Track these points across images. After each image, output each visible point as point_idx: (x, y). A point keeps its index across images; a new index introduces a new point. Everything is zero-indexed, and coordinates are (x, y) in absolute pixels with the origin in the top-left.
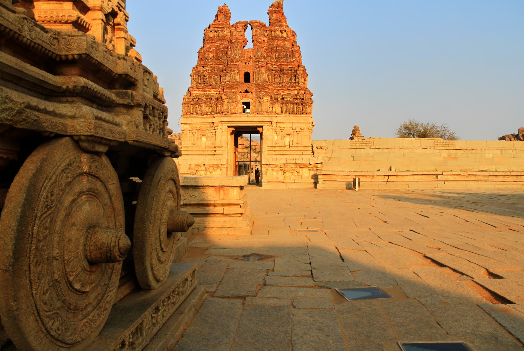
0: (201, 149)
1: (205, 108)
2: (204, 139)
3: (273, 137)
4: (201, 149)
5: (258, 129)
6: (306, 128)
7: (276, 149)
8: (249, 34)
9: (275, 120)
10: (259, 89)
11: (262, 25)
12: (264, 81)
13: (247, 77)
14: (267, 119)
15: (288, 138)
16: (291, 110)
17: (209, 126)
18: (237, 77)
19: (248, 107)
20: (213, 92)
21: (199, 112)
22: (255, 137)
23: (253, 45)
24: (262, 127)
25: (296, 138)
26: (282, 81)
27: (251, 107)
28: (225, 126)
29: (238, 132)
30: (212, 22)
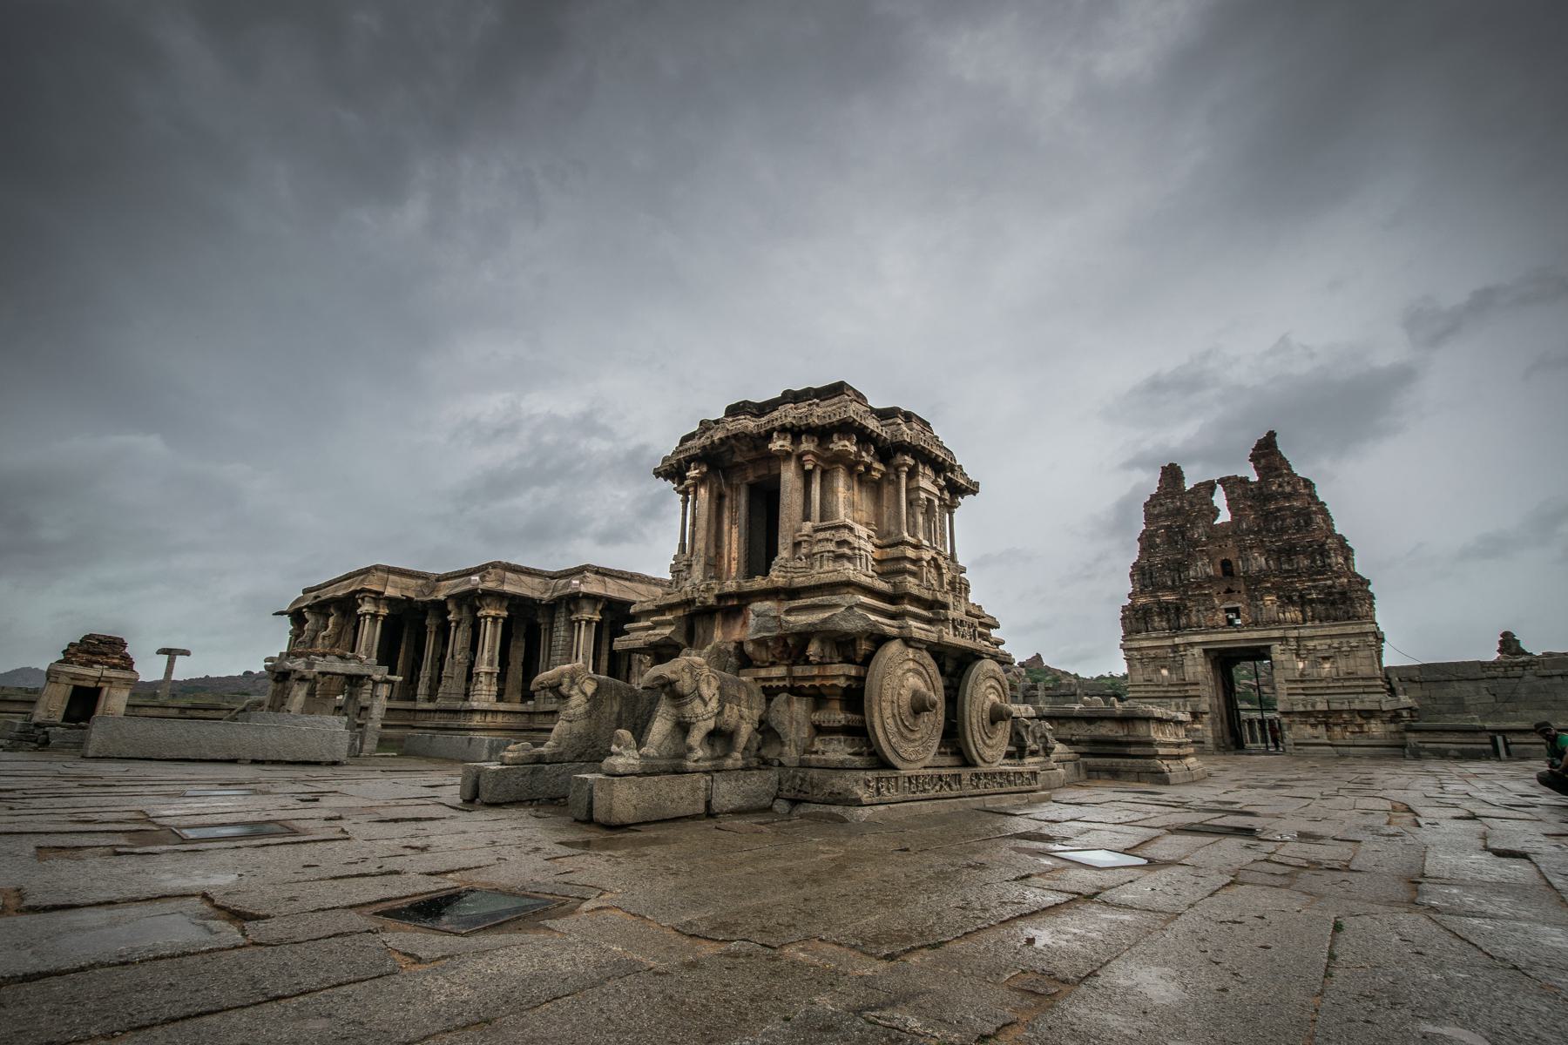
2: (1165, 672)
8: (1220, 499)
9: (1295, 633)
11: (1244, 481)
13: (1227, 567)
14: (1276, 634)
15: (1327, 666)
20: (1170, 598)
25: (1342, 664)
28: (1197, 651)
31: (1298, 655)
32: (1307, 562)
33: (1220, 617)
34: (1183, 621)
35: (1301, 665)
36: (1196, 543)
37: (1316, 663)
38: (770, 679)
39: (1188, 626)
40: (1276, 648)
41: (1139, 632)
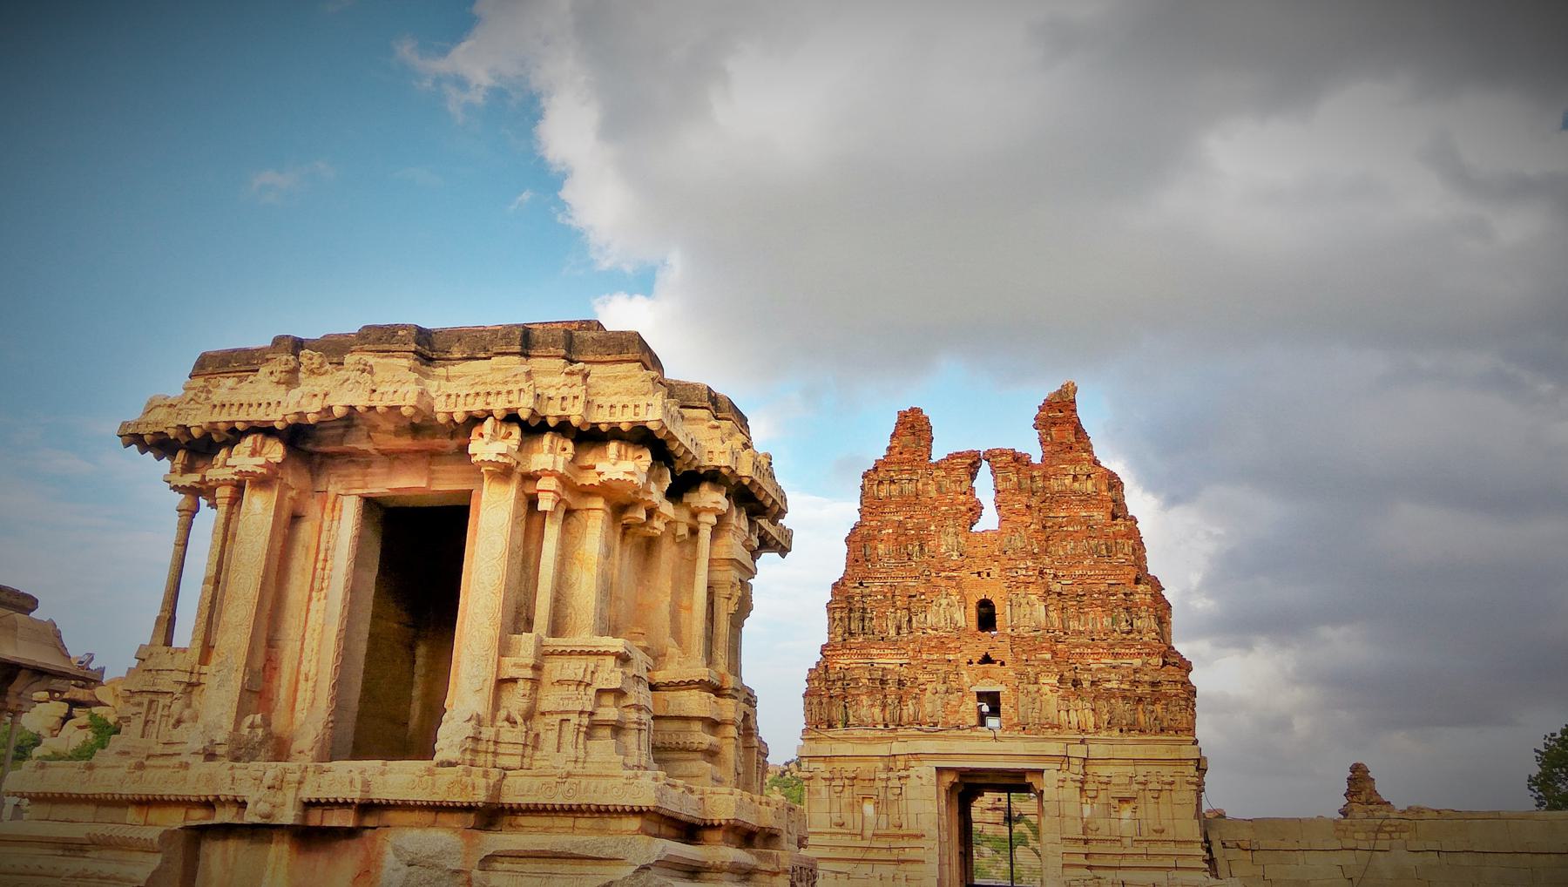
1: (867, 708)
5: (1028, 779)
6: (1177, 779)
7: (1093, 847)
8: (984, 486)
9: (1078, 751)
11: (1019, 460)
13: (987, 617)
14: (1054, 748)
15: (1126, 812)
16: (1129, 718)
17: (881, 765)
19: (995, 711)
21: (852, 720)
22: (1023, 804)
23: (997, 518)
24: (1041, 772)
27: (1003, 706)
28: (927, 770)
29: (966, 787)
30: (881, 453)
31: (1082, 790)
33: (970, 708)
34: (909, 709)
39: (917, 722)
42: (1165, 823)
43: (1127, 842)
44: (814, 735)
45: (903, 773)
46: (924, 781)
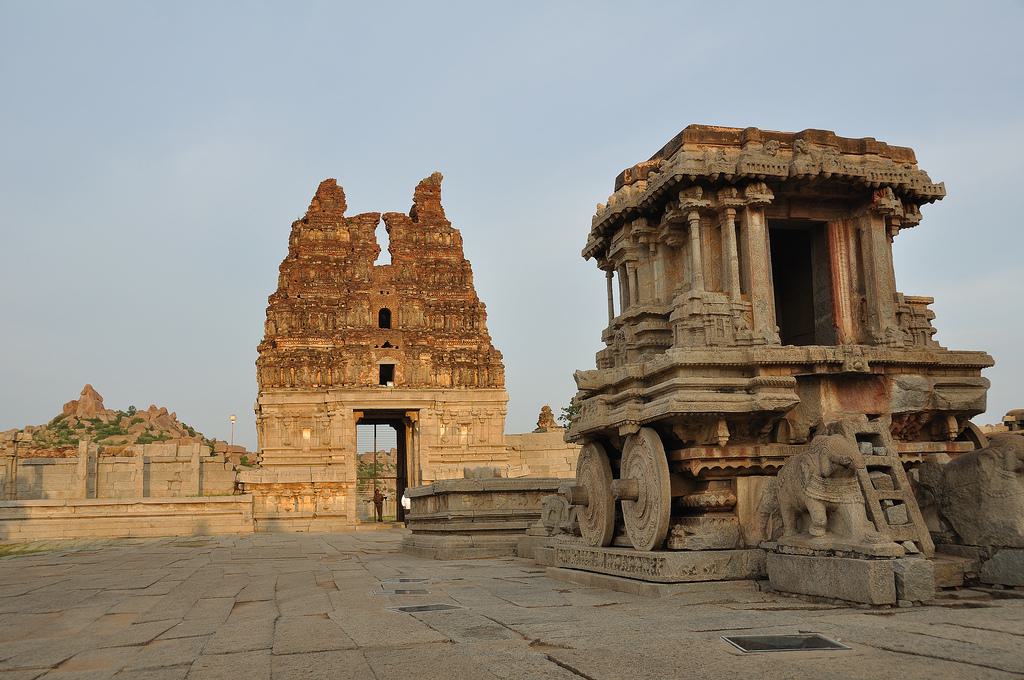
0: (301, 454)
2: (307, 434)
3: (438, 430)
4: (301, 454)
5: (408, 414)
8: (382, 236)
9: (441, 398)
10: (411, 340)
12: (419, 325)
13: (385, 318)
15: (464, 432)
16: (469, 380)
17: (316, 409)
18: (367, 317)
20: (322, 345)
21: (297, 382)
25: (477, 430)
26: (448, 326)
27: (397, 373)
28: (348, 411)
32: (459, 323)
33: (375, 375)
35: (442, 431)
36: (358, 285)
37: (455, 430)
38: (916, 454)
40: (425, 410)
41: (282, 386)
42: (486, 436)
43: (464, 447)
44: (271, 390)
45: (333, 413)
46: (346, 417)
